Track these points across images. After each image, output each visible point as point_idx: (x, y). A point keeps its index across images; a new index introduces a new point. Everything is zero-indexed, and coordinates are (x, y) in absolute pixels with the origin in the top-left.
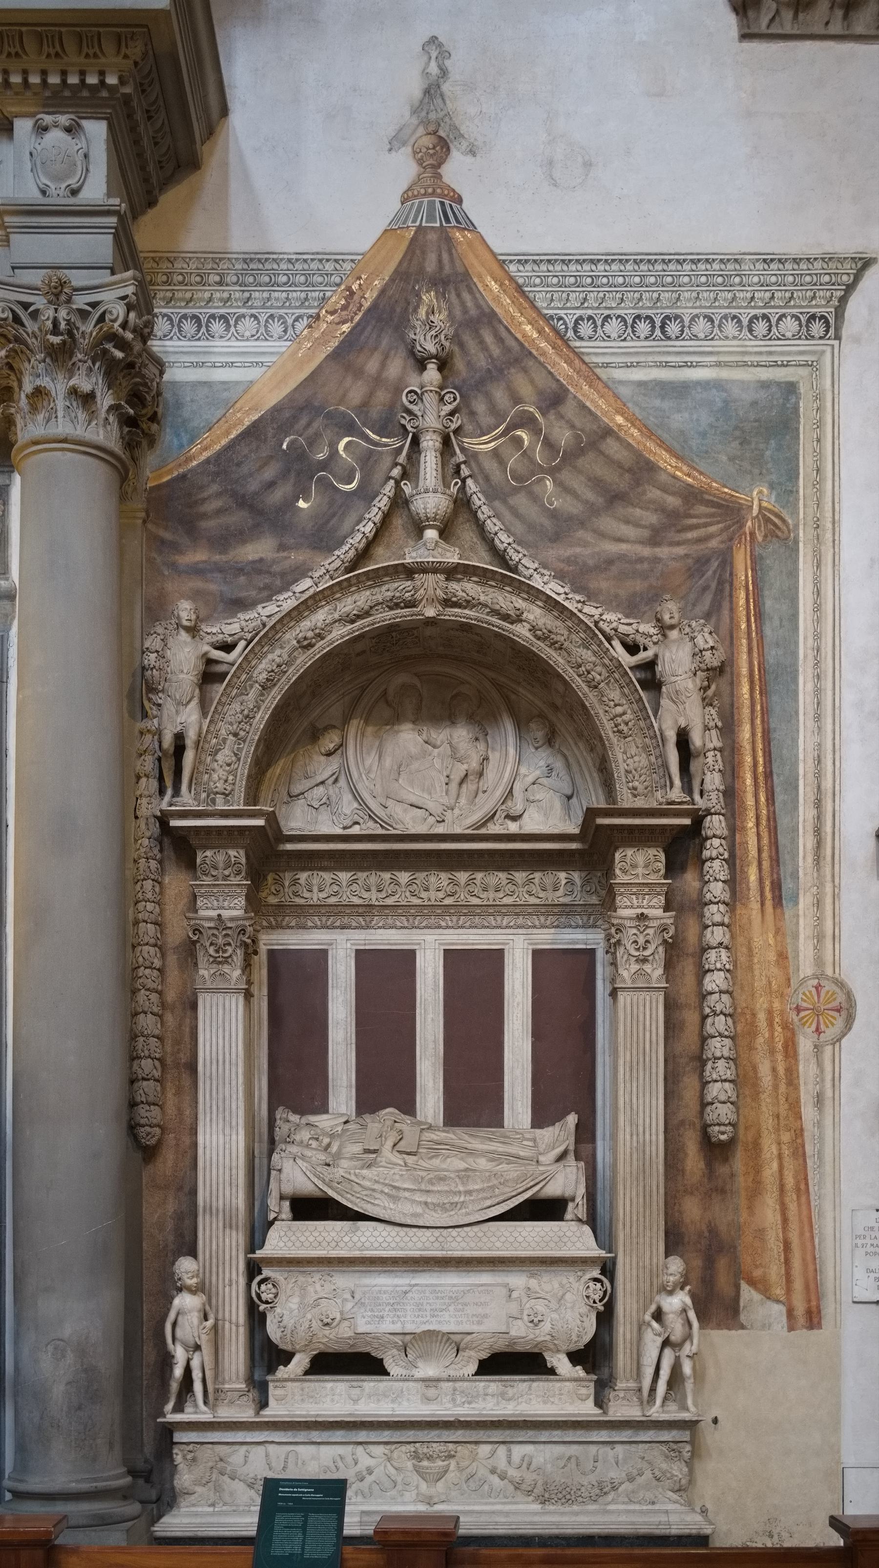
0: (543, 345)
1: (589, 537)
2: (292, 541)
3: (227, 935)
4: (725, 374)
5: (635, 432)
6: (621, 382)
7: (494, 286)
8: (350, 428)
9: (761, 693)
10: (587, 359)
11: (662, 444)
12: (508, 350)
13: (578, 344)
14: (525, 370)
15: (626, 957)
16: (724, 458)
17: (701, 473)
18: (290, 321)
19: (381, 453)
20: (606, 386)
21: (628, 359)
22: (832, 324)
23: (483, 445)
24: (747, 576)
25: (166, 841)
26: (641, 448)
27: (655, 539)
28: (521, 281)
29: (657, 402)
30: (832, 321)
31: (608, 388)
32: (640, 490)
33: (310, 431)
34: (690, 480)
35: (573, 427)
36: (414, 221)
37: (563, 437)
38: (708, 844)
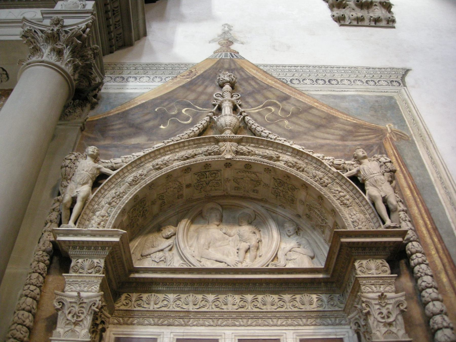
0: (278, 85)
1: (310, 138)
2: (155, 138)
3: (83, 307)
4: (360, 93)
5: (325, 108)
6: (315, 95)
7: (255, 72)
8: (188, 105)
9: (417, 194)
10: (298, 89)
11: (338, 111)
12: (262, 86)
13: (293, 85)
14: (270, 91)
15: (376, 323)
16: (369, 116)
17: (360, 120)
18: (163, 78)
19: (203, 113)
20: (308, 95)
21: (317, 89)
22: (402, 82)
23: (253, 111)
24: (393, 152)
25: (55, 259)
26: (328, 112)
27: (343, 138)
28: (265, 70)
29: (333, 100)
30: (401, 82)
31: (309, 96)
32: (332, 124)
33: (169, 106)
34: (355, 122)
35: (295, 105)
36: (220, 56)
37: (291, 108)
38: (414, 256)
